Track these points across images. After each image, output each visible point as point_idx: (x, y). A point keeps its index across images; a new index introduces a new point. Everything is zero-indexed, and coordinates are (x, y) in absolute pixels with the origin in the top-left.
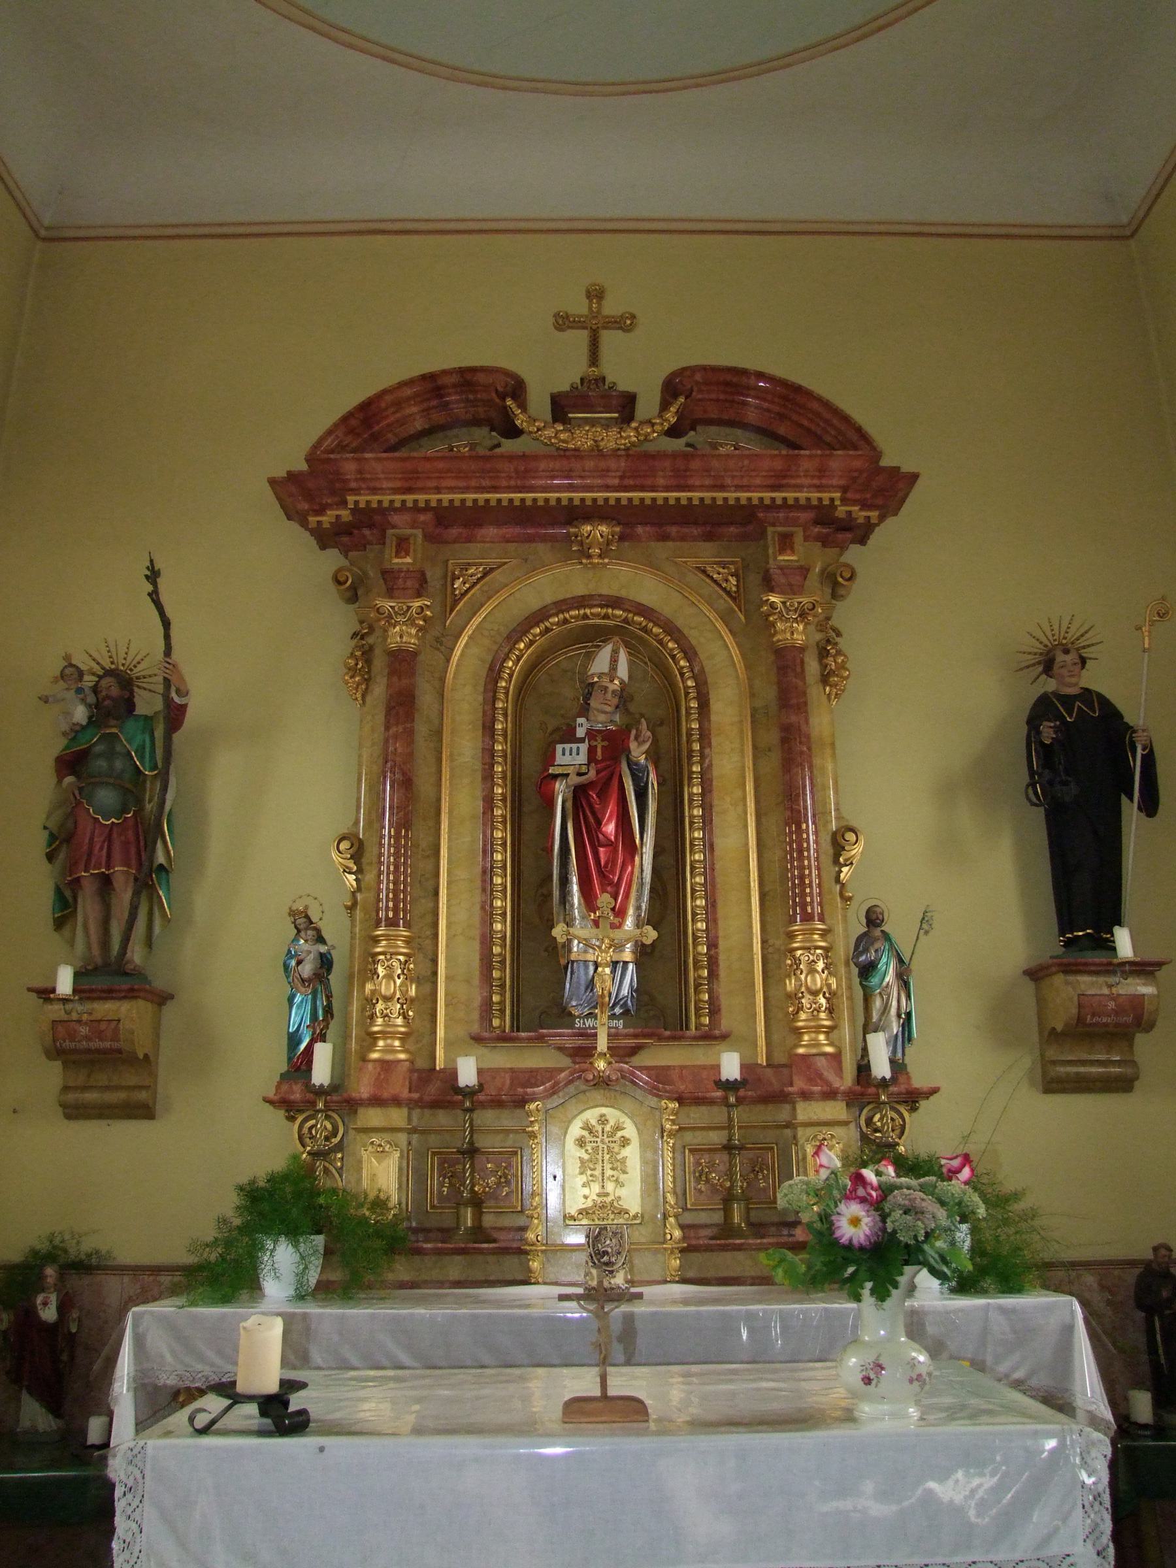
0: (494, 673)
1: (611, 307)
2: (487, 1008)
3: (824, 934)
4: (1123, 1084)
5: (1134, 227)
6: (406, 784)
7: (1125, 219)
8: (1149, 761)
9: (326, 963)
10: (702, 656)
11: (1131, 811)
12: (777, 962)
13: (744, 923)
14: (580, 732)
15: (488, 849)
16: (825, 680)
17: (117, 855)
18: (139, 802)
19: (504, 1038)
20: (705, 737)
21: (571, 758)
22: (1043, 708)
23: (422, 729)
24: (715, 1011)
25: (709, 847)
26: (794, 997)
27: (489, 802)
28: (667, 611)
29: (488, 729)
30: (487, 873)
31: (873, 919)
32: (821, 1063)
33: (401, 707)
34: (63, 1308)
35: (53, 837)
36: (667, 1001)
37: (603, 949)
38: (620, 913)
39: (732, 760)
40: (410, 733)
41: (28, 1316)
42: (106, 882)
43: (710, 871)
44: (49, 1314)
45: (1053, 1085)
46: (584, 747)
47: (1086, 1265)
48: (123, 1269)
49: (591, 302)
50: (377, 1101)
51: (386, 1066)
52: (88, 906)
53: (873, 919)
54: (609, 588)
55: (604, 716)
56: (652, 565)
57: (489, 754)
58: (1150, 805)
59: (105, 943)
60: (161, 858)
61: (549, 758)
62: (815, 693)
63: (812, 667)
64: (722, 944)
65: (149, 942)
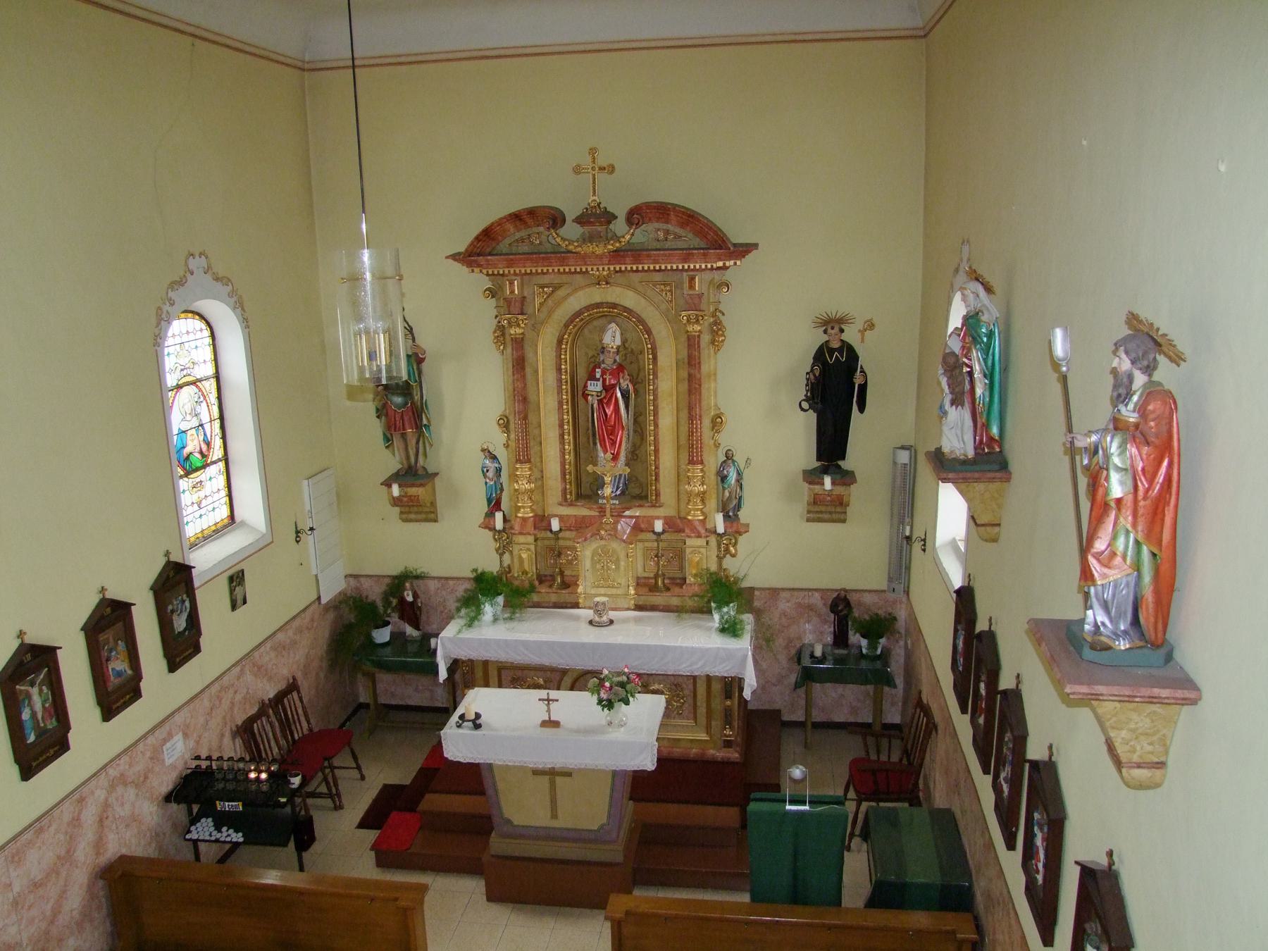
0: (560, 342)
1: (602, 161)
2: (564, 491)
3: (702, 470)
4: (844, 521)
5: (927, 29)
6: (525, 400)
7: (921, 25)
8: (863, 388)
9: (499, 471)
10: (654, 332)
11: (855, 407)
12: (680, 478)
13: (667, 460)
14: (598, 376)
15: (561, 426)
16: (713, 342)
17: (407, 425)
18: (412, 398)
19: (571, 505)
20: (655, 375)
21: (595, 387)
22: (821, 355)
23: (528, 370)
24: (658, 495)
25: (656, 425)
26: (690, 494)
27: (560, 403)
28: (637, 309)
29: (559, 370)
30: (562, 436)
31: (729, 457)
32: (697, 523)
33: (520, 365)
34: (415, 596)
35: (378, 410)
36: (637, 490)
37: (610, 468)
38: (615, 458)
39: (667, 384)
40: (524, 377)
41: (402, 600)
42: (404, 436)
43: (656, 436)
44: (410, 599)
45: (808, 520)
46: (600, 383)
47: (816, 590)
48: (434, 578)
49: (501, 555)
50: (521, 533)
51: (524, 520)
52: (397, 441)
53: (729, 457)
54: (611, 299)
55: (609, 361)
56: (629, 287)
57: (560, 380)
58: (862, 409)
59: (408, 458)
60: (425, 421)
61: (585, 386)
62: (706, 351)
63: (706, 338)
64: (661, 467)
65: (425, 455)
